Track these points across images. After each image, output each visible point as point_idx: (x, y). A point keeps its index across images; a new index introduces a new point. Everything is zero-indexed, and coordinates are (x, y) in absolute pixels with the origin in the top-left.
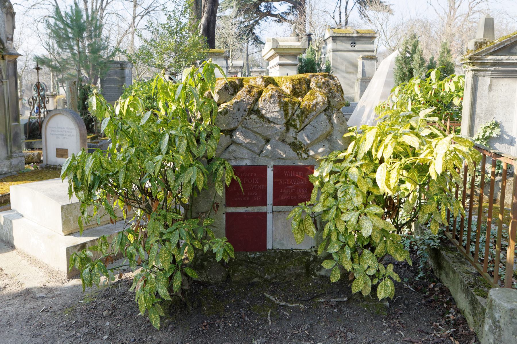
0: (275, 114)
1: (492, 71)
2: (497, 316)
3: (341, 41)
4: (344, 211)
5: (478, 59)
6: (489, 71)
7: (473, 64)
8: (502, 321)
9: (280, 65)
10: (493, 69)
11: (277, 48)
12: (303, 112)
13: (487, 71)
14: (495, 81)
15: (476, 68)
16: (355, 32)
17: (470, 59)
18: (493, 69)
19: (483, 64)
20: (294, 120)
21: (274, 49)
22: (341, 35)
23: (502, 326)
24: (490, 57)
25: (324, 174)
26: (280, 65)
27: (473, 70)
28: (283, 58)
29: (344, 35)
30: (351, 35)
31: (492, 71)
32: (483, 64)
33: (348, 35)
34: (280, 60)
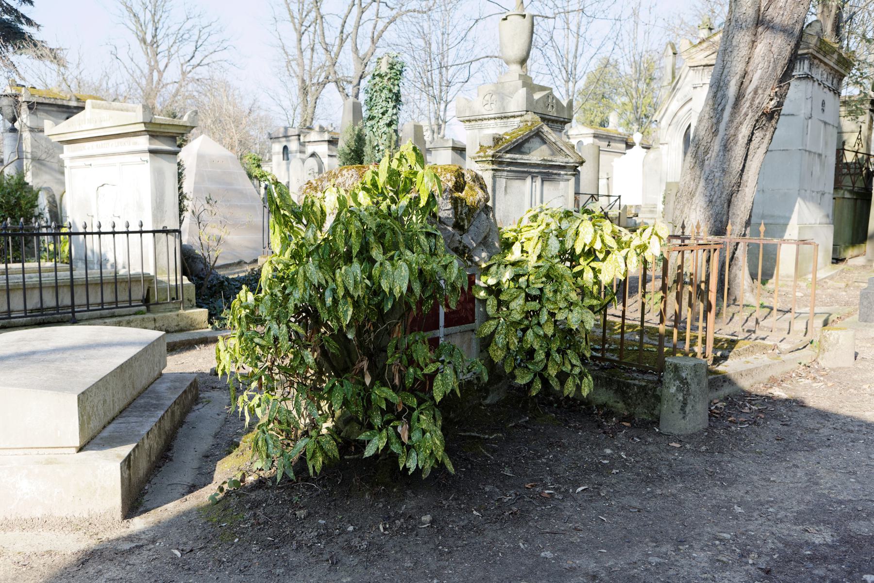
0: (67, 248)
1: (508, 171)
2: (684, 375)
3: (46, 112)
4: (556, 311)
5: (500, 157)
6: (504, 170)
7: (493, 162)
8: (689, 377)
9: (152, 152)
10: (508, 169)
11: (151, 122)
12: (469, 210)
13: (504, 170)
14: (509, 182)
15: (495, 167)
16: (73, 98)
17: (493, 156)
18: (508, 169)
19: (501, 163)
20: (463, 220)
21: (145, 123)
22: (47, 101)
23: (689, 381)
24: (508, 156)
25: (504, 280)
26: (152, 152)
27: (493, 170)
28: (156, 141)
29: (52, 101)
30: (65, 103)
31: (508, 171)
32: (501, 163)
33: (59, 102)
34: (150, 144)
